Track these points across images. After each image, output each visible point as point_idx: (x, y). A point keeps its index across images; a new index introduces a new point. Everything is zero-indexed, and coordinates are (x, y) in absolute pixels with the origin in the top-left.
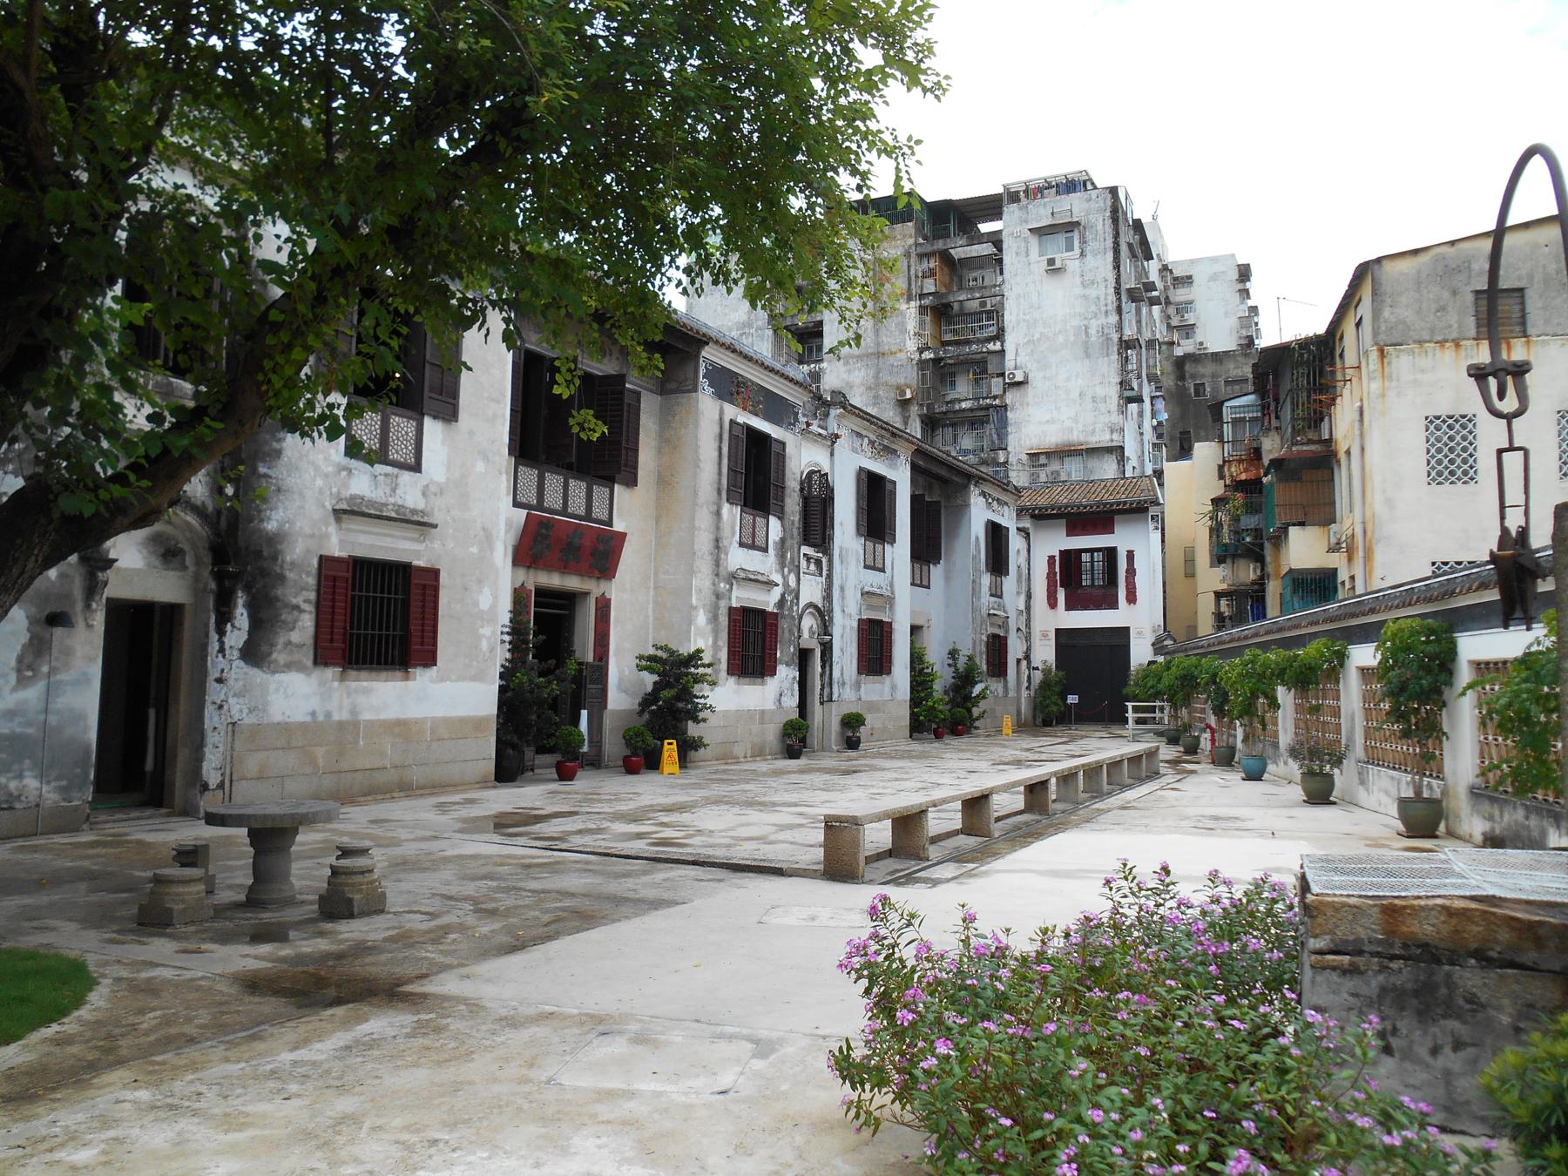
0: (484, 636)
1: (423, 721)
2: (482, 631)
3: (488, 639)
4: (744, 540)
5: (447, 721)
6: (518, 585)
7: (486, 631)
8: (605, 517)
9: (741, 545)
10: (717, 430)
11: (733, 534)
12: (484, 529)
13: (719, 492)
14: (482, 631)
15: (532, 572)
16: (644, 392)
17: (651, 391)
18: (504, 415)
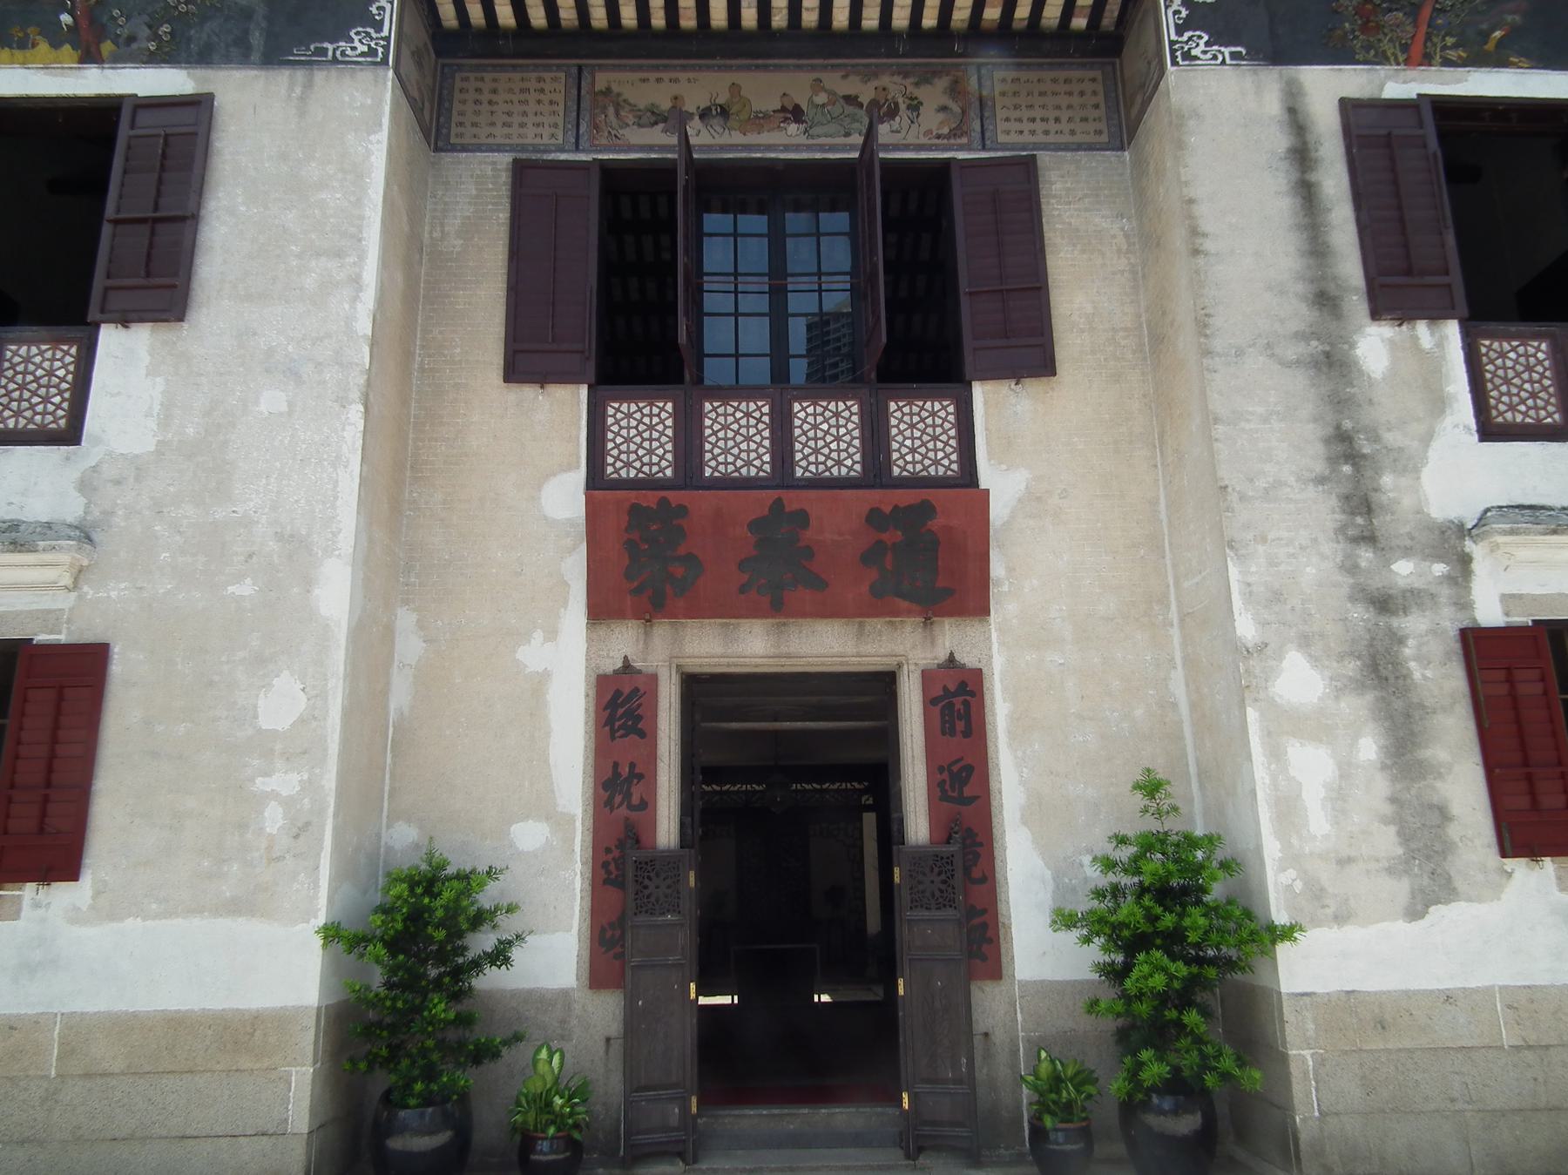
0: (274, 795)
1: (37, 1023)
2: (262, 784)
3: (288, 803)
4: (1503, 414)
5: (123, 1026)
6: (612, 664)
7: (284, 782)
8: (947, 463)
9: (1490, 431)
10: (1281, 141)
11: (1439, 404)
12: (279, 537)
13: (1325, 300)
14: (262, 784)
15: (662, 631)
16: (1044, 158)
17: (1090, 147)
18: (356, 281)
